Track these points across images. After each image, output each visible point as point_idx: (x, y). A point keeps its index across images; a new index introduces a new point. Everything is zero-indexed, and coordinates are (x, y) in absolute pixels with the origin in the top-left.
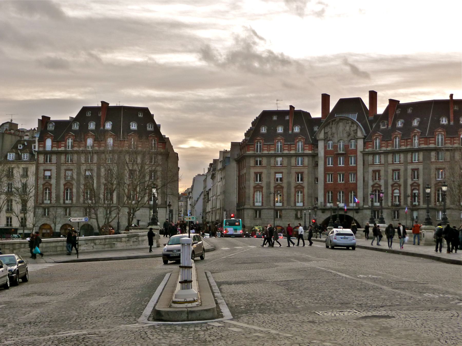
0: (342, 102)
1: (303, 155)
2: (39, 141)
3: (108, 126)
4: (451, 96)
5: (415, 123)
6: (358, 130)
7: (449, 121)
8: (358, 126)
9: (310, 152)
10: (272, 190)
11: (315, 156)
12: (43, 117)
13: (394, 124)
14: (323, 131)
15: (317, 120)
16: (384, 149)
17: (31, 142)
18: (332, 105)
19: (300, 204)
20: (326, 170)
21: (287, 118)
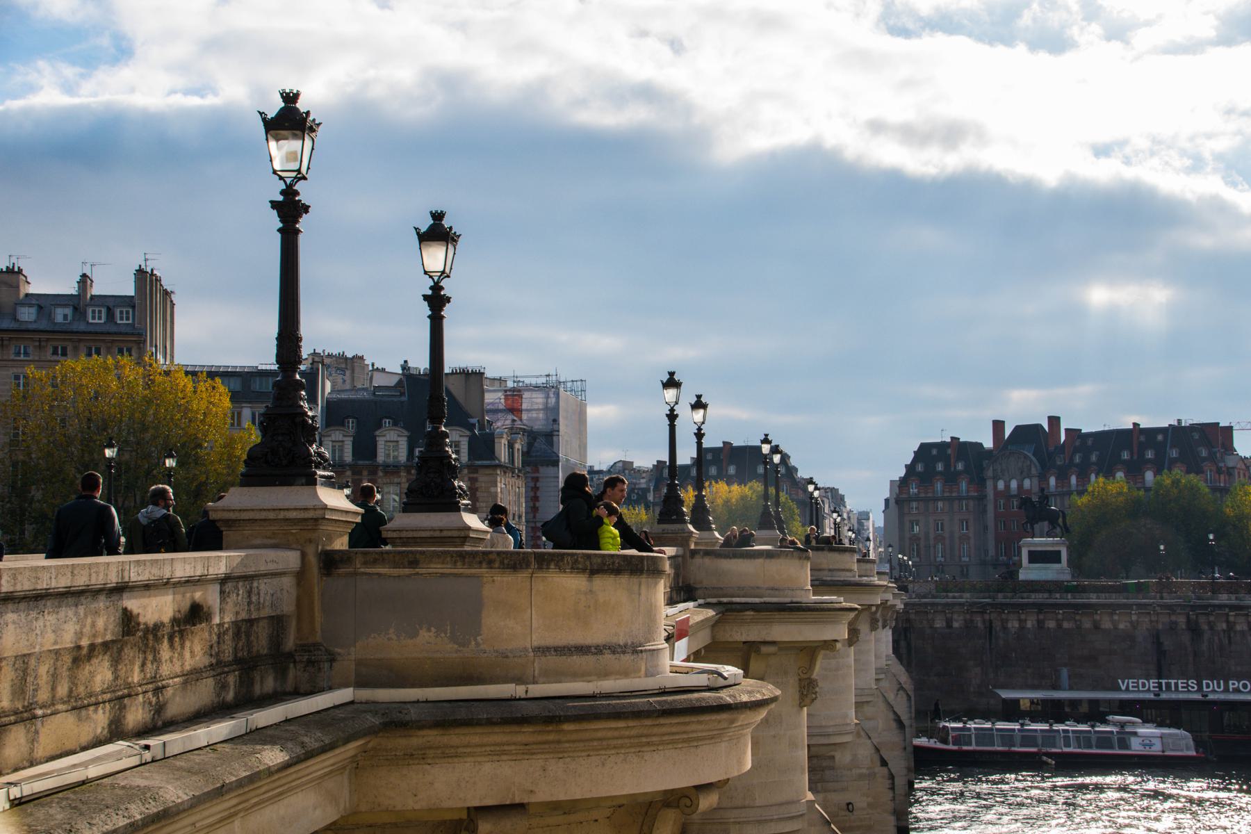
0: (1018, 429)
1: (968, 498)
2: (654, 491)
6: (1032, 466)
7: (1132, 454)
8: (1031, 461)
9: (976, 494)
10: (932, 542)
11: (982, 498)
12: (658, 462)
13: (1071, 459)
14: (991, 468)
15: (989, 452)
16: (1060, 489)
17: (646, 490)
18: (1008, 432)
19: (966, 559)
20: (997, 516)
21: (949, 451)
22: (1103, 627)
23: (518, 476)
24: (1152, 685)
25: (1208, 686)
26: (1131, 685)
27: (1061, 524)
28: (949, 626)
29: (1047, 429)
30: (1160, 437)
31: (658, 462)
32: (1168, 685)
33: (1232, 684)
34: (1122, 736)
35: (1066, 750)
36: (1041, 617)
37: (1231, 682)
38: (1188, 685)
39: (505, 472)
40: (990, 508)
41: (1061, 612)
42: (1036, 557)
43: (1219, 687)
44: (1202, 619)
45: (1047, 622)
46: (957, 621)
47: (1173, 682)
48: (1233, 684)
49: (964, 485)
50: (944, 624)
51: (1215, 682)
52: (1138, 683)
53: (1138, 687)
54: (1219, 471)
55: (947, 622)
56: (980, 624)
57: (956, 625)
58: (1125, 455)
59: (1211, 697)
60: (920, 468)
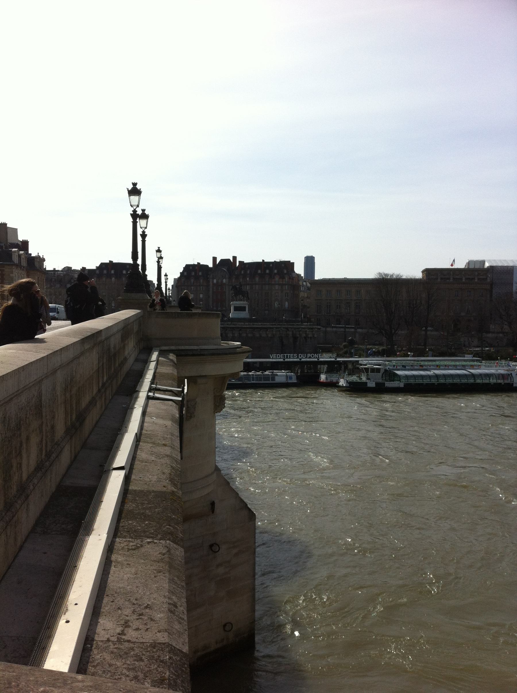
0: (222, 261)
3: (113, 272)
4: (263, 260)
5: (248, 272)
7: (261, 271)
9: (206, 284)
15: (211, 268)
18: (218, 261)
23: (23, 270)
24: (281, 356)
25: (300, 356)
26: (274, 356)
29: (232, 261)
31: (82, 267)
32: (287, 356)
33: (308, 356)
34: (273, 376)
35: (252, 382)
37: (308, 354)
38: (294, 356)
39: (17, 268)
40: (211, 289)
42: (237, 309)
47: (289, 355)
48: (309, 355)
49: (202, 281)
52: (277, 356)
53: (276, 357)
54: (290, 278)
58: (259, 271)
59: (303, 360)
60: (185, 274)
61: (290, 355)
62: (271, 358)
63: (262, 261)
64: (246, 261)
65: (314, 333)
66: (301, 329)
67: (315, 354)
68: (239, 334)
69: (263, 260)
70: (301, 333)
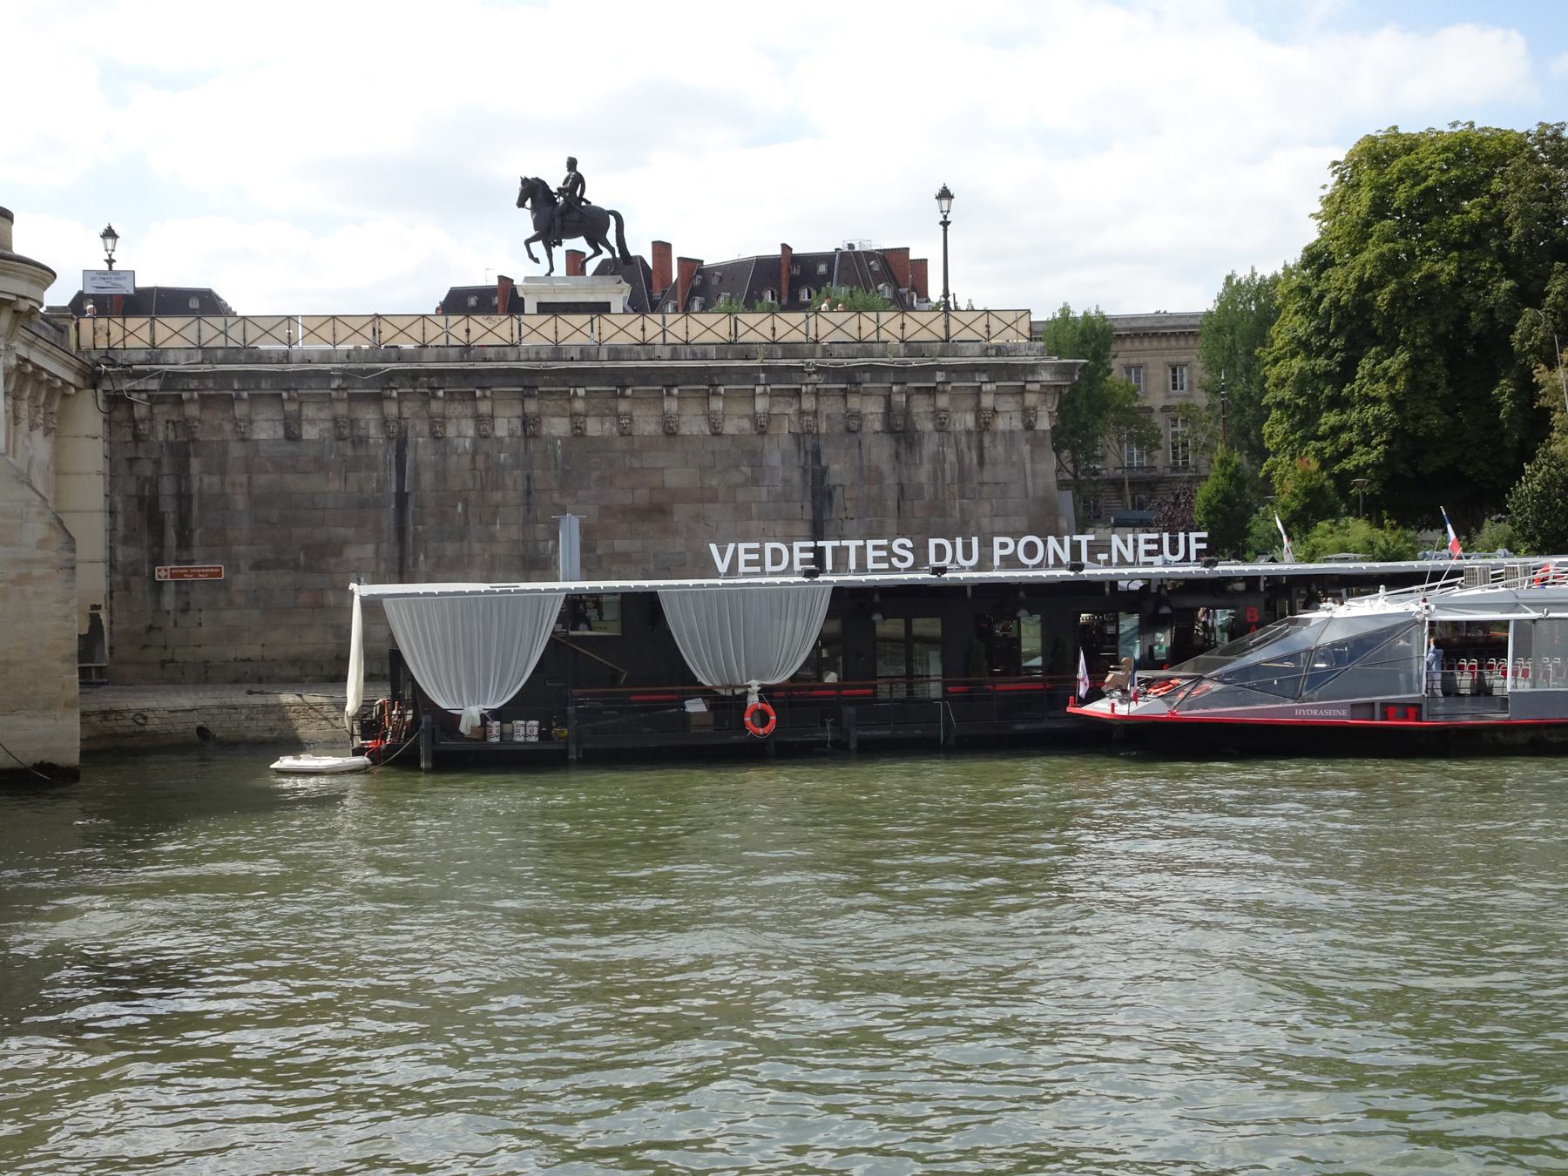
22: (685, 430)
24: (797, 556)
26: (742, 557)
27: (613, 243)
28: (292, 436)
30: (822, 268)
32: (840, 553)
36: (532, 406)
37: (997, 541)
38: (891, 554)
41: (581, 392)
43: (968, 556)
44: (921, 406)
45: (545, 421)
46: (312, 422)
47: (852, 544)
48: (1004, 546)
50: (281, 433)
51: (959, 541)
52: (761, 551)
53: (761, 563)
55: (287, 428)
56: (374, 432)
57: (310, 433)
61: (861, 551)
62: (717, 575)
63: (778, 252)
64: (710, 260)
65: (1030, 400)
66: (940, 377)
67: (1052, 540)
68: (525, 420)
69: (786, 248)
70: (943, 401)
